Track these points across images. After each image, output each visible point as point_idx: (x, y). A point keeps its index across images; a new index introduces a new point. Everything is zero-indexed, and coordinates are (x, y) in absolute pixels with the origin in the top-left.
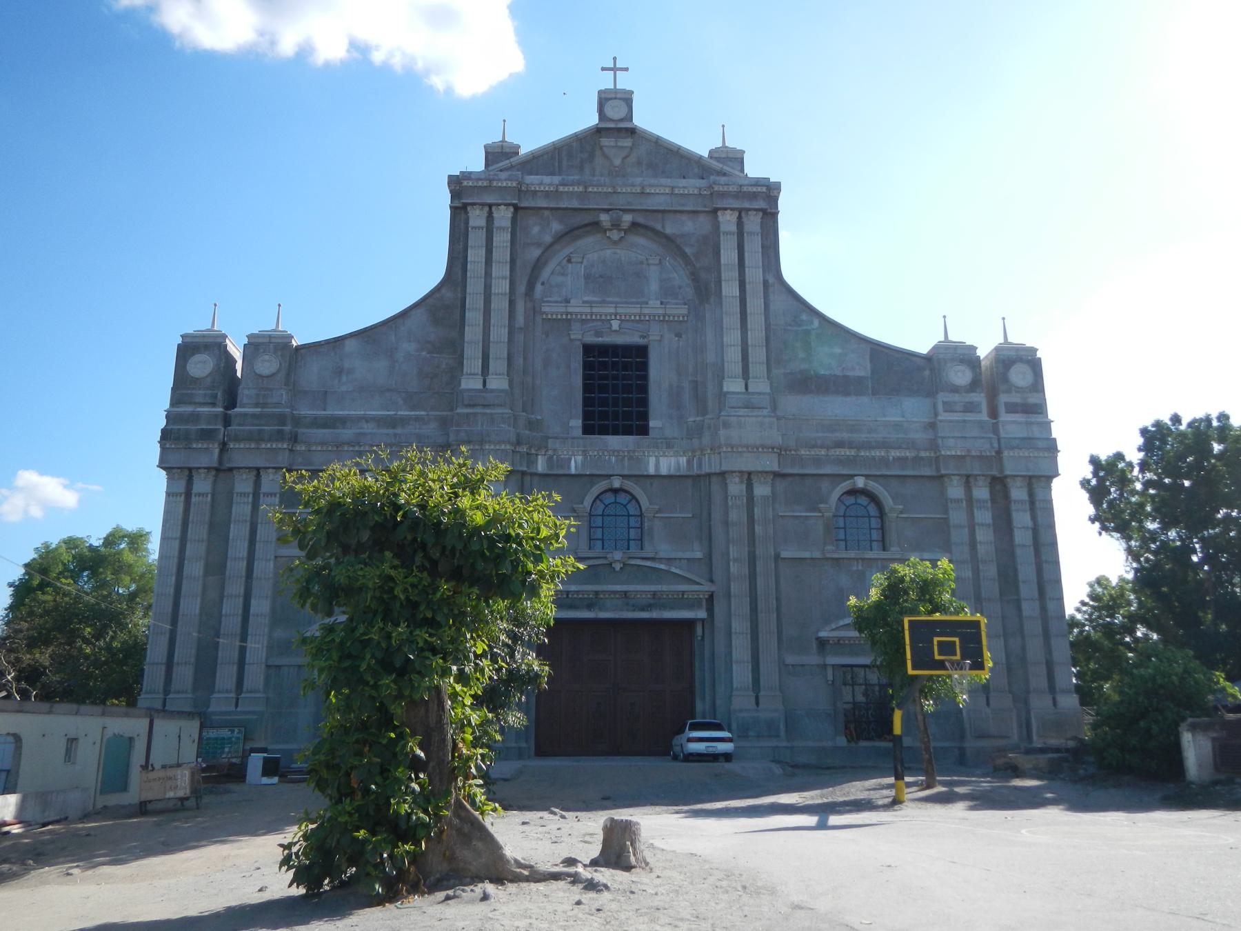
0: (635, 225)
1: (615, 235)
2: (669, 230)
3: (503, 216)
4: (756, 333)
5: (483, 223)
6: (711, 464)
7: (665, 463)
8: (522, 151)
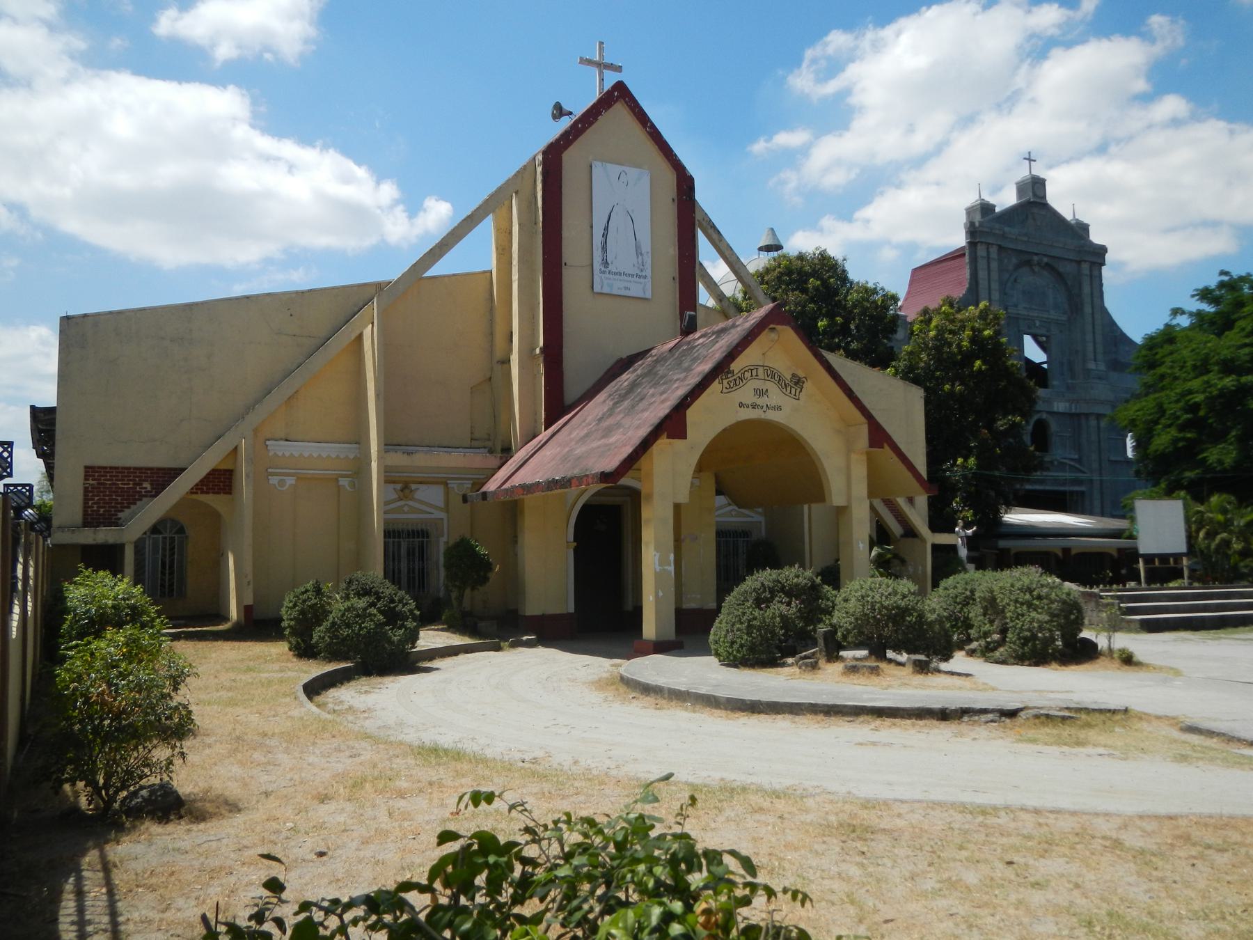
0: (1047, 264)
1: (1037, 269)
2: (1061, 270)
3: (994, 250)
4: (1099, 338)
5: (985, 254)
6: (1084, 409)
7: (1060, 406)
8: (997, 210)
